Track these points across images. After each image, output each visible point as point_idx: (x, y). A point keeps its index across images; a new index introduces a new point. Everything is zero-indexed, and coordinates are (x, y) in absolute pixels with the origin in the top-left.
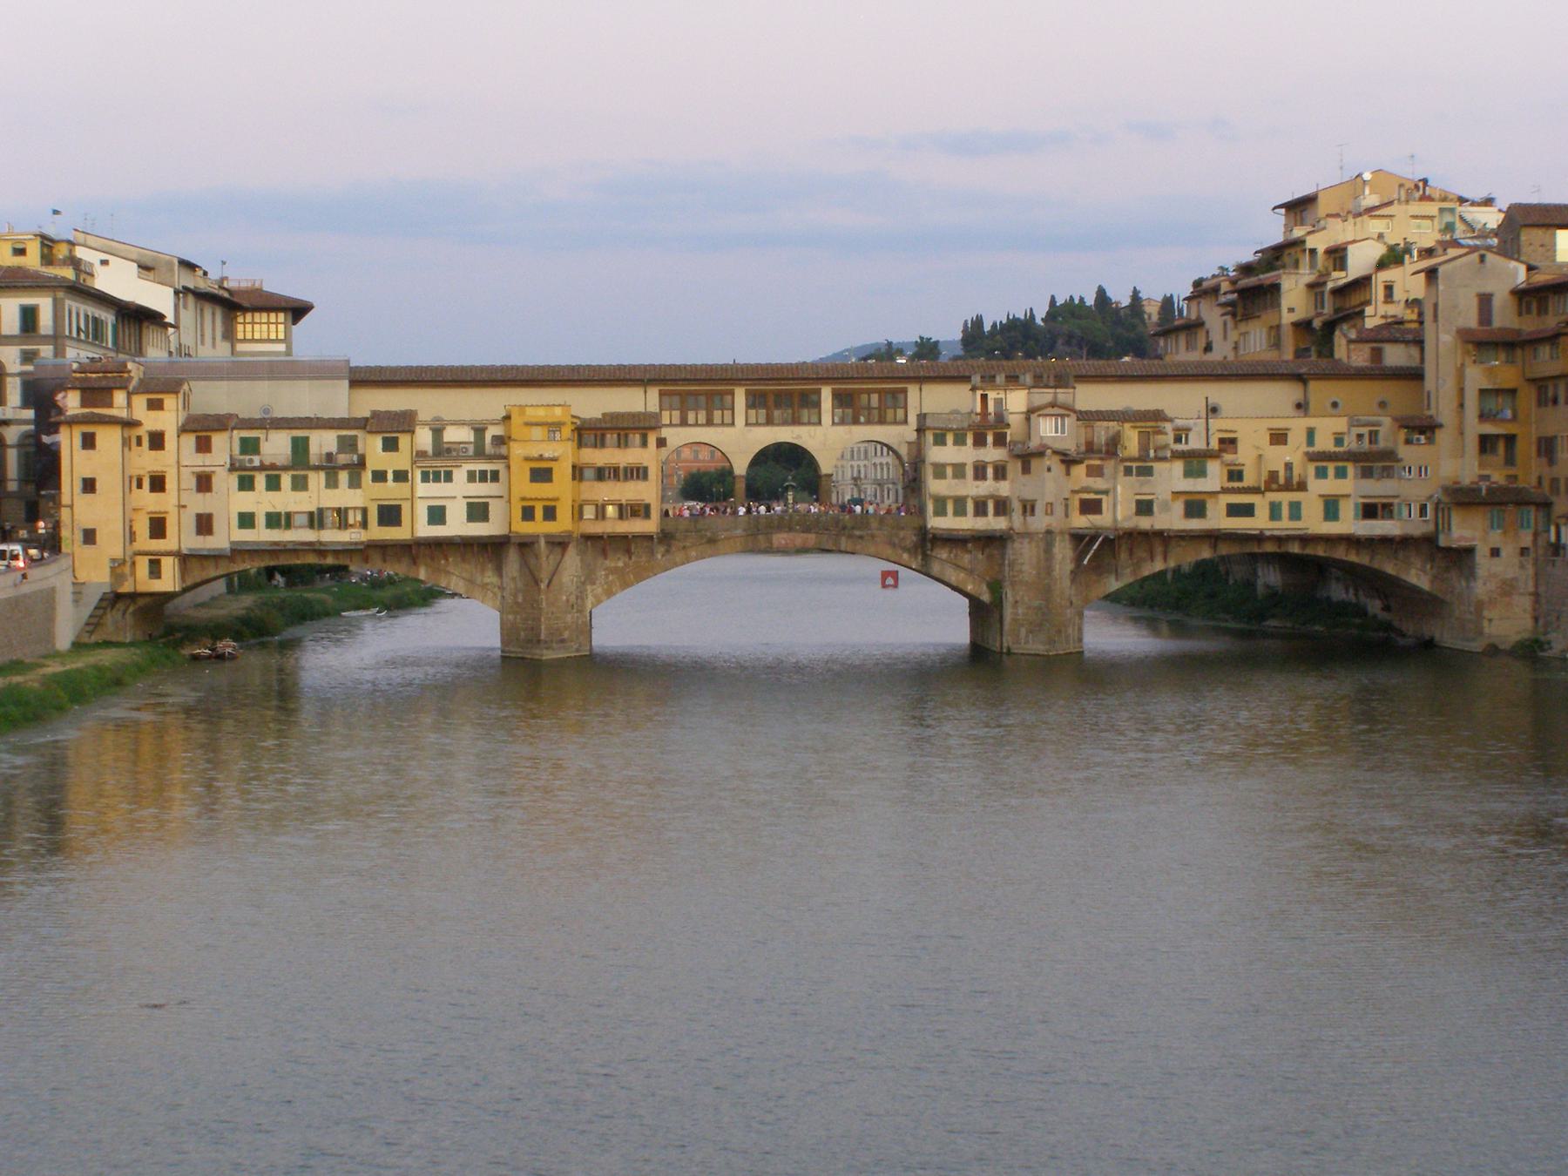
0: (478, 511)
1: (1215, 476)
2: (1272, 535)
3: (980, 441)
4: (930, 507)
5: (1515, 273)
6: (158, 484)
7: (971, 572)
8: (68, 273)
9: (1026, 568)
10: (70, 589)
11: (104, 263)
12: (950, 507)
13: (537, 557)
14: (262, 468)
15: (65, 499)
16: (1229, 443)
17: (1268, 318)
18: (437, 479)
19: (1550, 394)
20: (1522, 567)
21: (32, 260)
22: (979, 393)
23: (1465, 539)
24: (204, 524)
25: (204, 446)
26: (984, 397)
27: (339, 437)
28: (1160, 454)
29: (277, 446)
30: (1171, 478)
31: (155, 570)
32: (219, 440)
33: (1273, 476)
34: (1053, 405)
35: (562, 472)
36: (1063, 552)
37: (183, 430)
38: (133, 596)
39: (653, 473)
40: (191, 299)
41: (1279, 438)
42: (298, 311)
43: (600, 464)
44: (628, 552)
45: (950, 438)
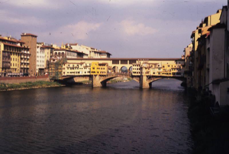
0: (89, 72)
1: (162, 70)
3: (138, 66)
7: (137, 79)
8: (68, 49)
16: (164, 67)
22: (138, 62)
32: (65, 65)
35: (96, 68)
40: (93, 52)
41: (169, 66)
44: (104, 77)
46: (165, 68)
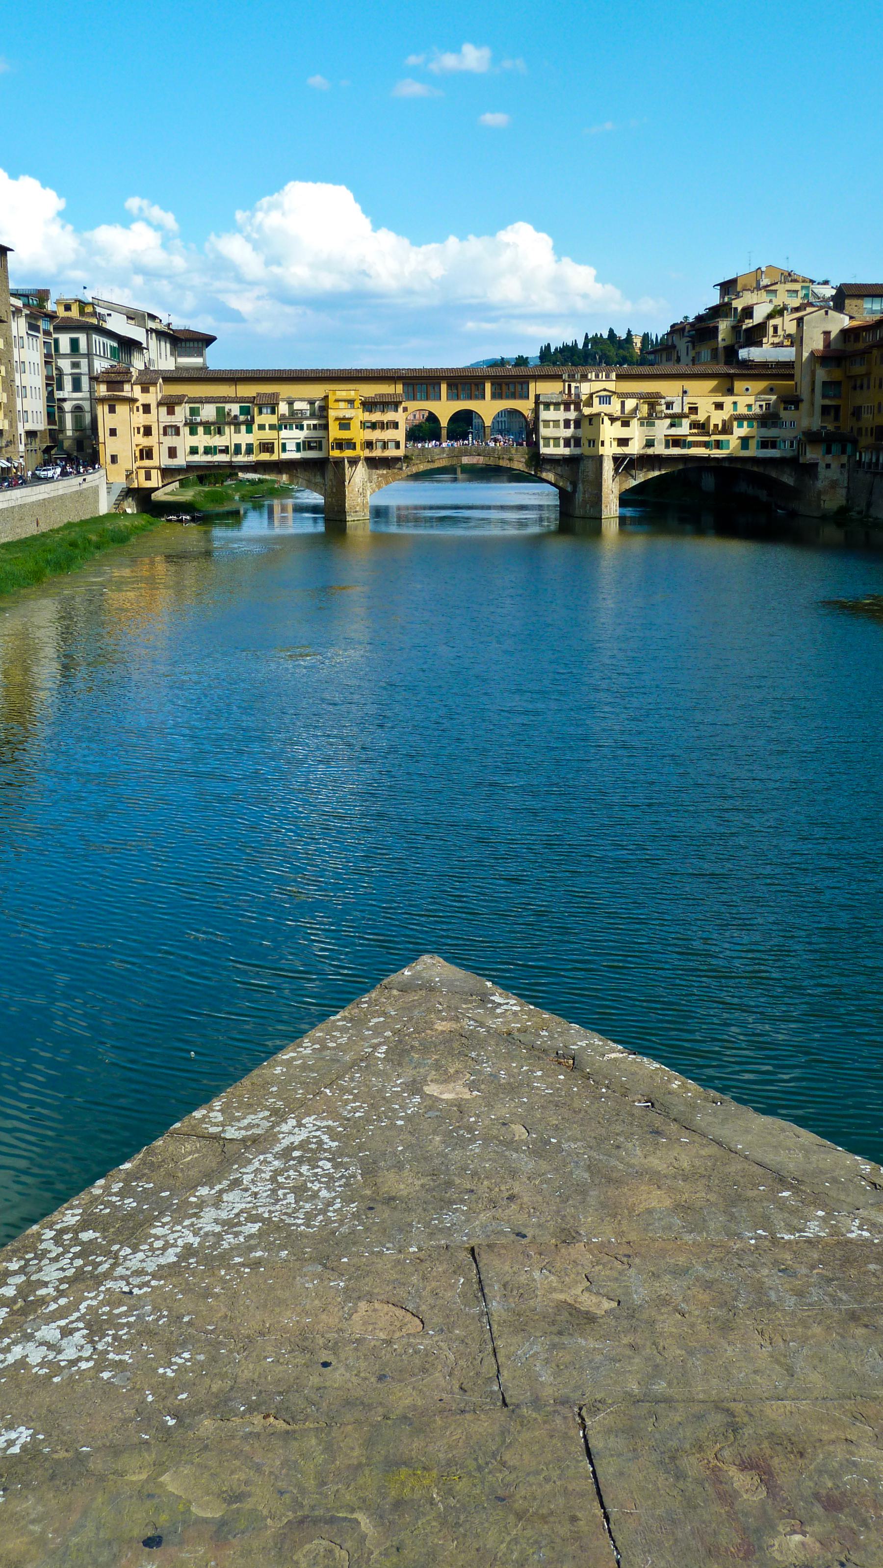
2: (715, 458)
3: (567, 409)
4: (541, 442)
5: (843, 321)
6: (148, 431)
8: (94, 321)
9: (590, 474)
10: (105, 486)
11: (109, 315)
12: (552, 442)
13: (344, 469)
14: (201, 423)
15: (101, 440)
16: (694, 410)
17: (712, 344)
18: (291, 429)
19: (859, 383)
20: (841, 473)
21: (74, 313)
22: (567, 384)
23: (814, 459)
24: (172, 452)
25: (171, 412)
26: (569, 386)
27: (241, 407)
28: (659, 415)
29: (208, 412)
30: (662, 429)
31: (148, 477)
33: (716, 426)
34: (605, 390)
35: (355, 424)
36: (608, 467)
37: (159, 404)
38: (138, 489)
39: (403, 426)
40: (154, 335)
41: (719, 406)
42: (209, 340)
43: (374, 421)
45: (552, 407)
46: (701, 417)
